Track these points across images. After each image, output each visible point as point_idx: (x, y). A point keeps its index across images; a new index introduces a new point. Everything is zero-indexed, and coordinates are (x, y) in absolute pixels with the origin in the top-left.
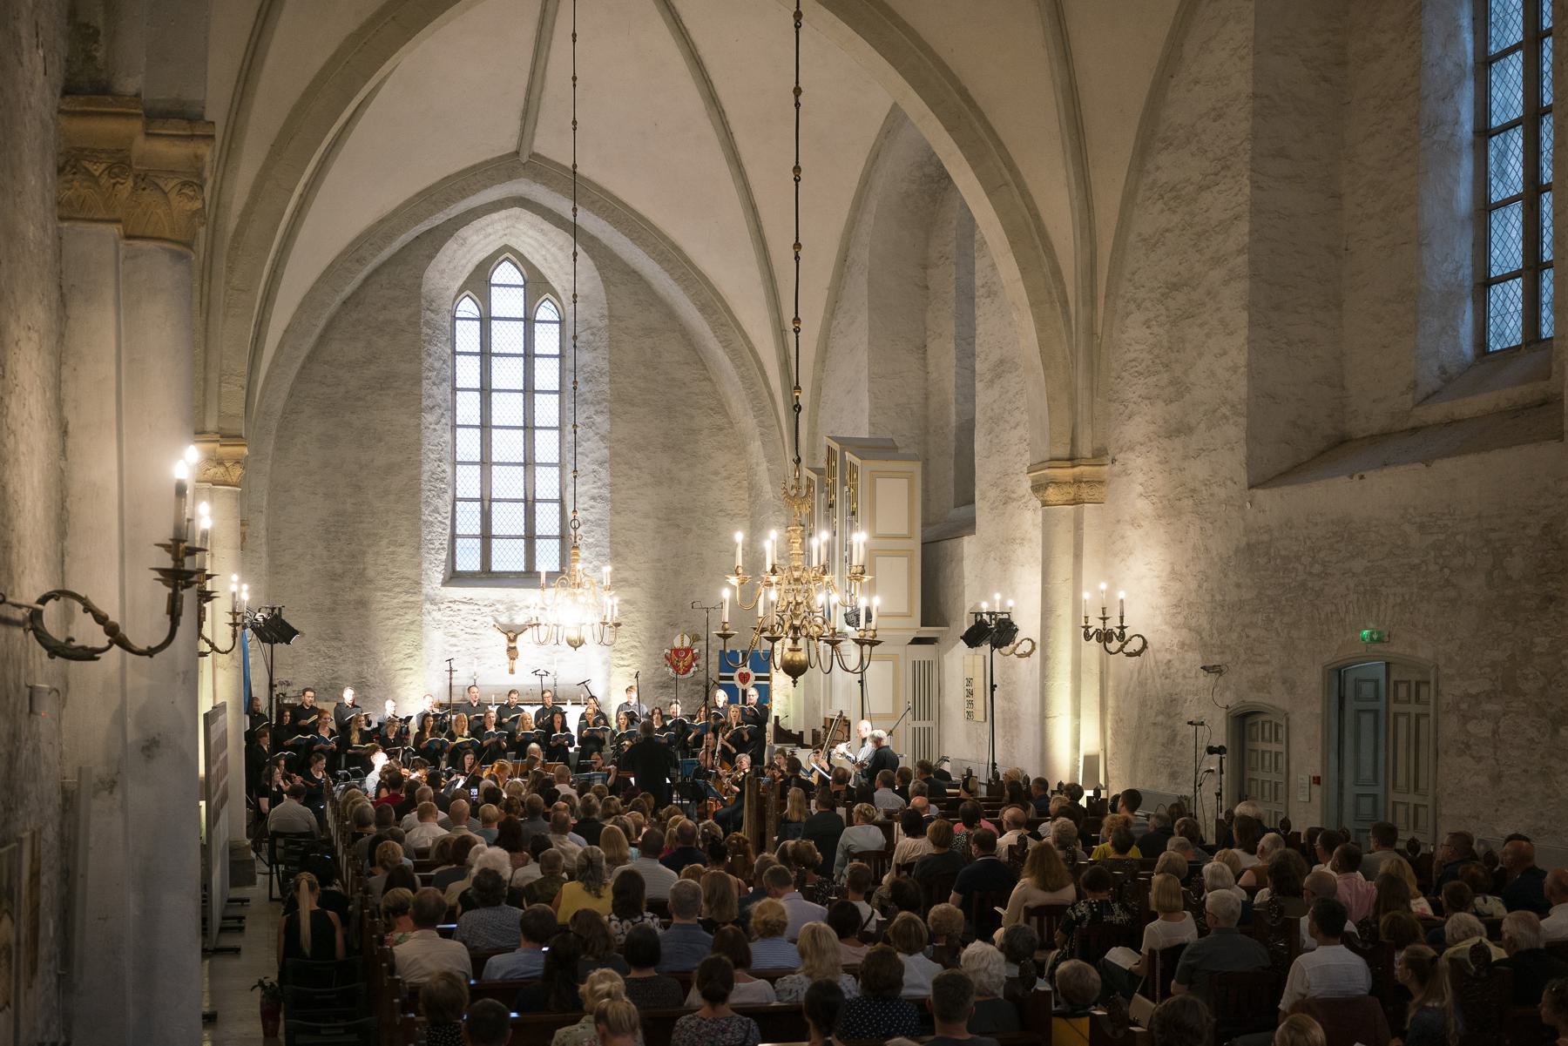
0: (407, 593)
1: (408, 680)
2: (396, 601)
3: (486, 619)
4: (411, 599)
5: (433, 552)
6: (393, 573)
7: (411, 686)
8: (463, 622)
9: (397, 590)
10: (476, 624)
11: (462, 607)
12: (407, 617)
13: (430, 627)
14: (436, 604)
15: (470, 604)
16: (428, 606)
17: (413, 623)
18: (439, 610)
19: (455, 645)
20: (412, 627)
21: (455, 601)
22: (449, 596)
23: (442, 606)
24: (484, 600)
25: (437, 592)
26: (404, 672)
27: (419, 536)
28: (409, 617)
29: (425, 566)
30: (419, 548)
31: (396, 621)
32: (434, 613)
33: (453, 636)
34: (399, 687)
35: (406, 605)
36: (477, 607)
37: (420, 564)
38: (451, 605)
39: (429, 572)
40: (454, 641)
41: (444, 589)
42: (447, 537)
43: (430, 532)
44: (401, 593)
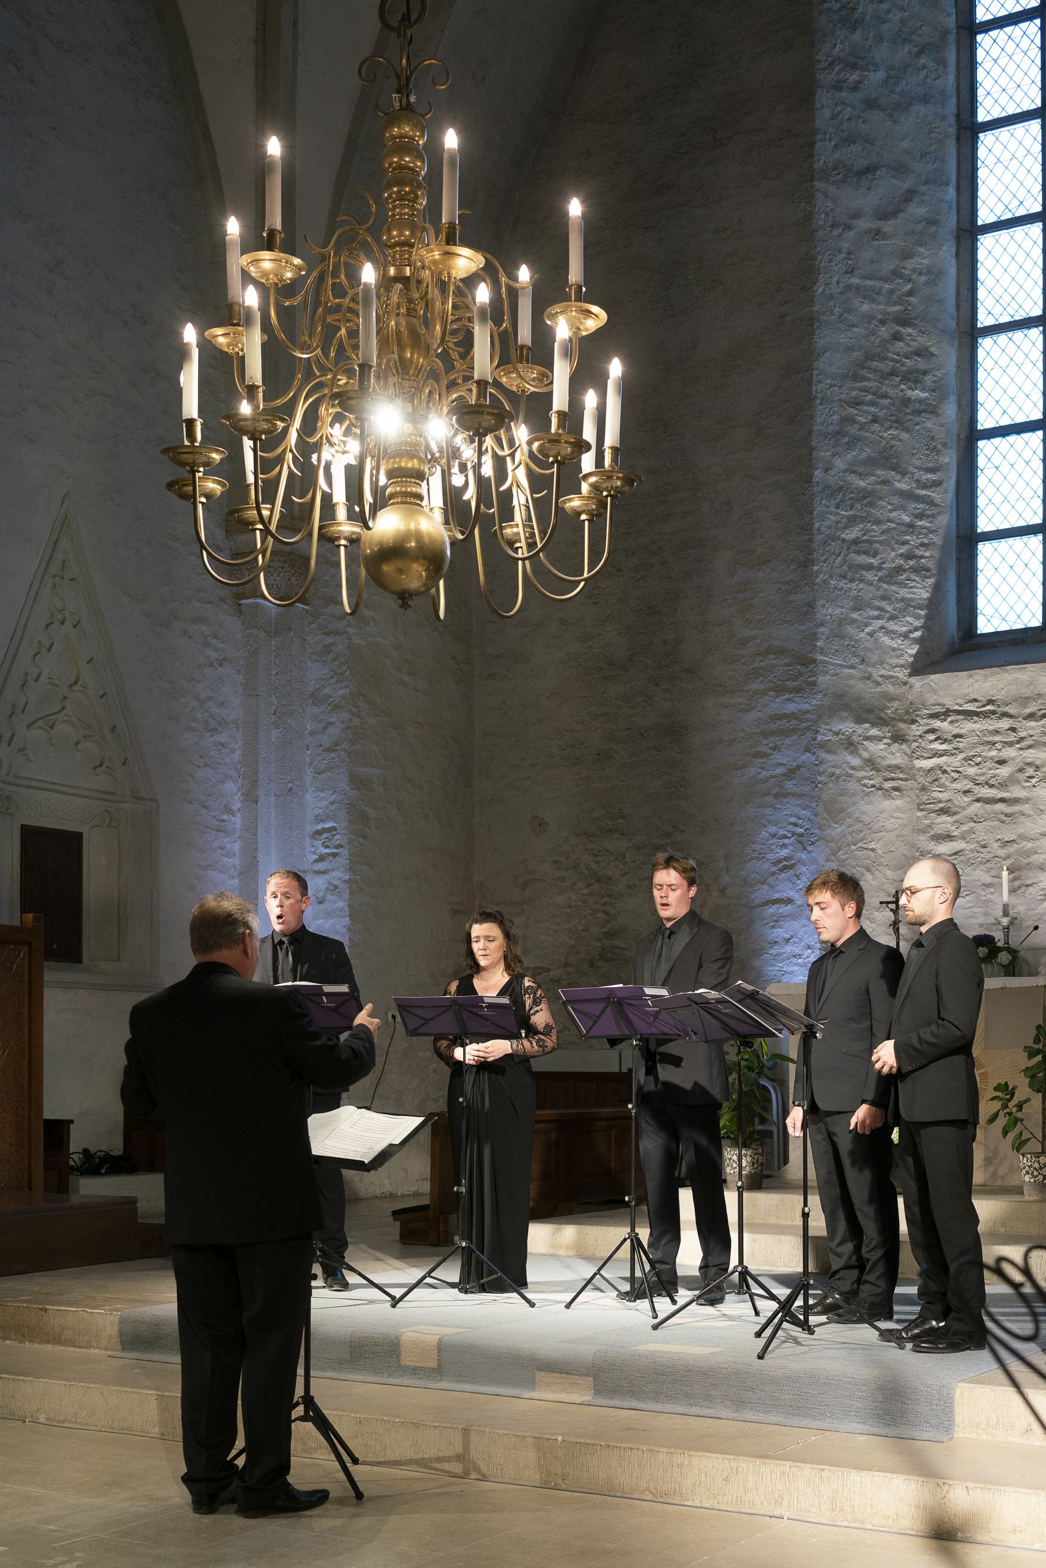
0: (779, 690)
1: (780, 933)
2: (754, 715)
3: (1031, 755)
4: (791, 708)
5: (869, 576)
6: (743, 643)
7: (788, 949)
8: (972, 771)
9: (756, 685)
10: (1004, 771)
11: (968, 726)
12: (778, 757)
13: (852, 785)
14: (881, 722)
15: (986, 715)
16: (848, 727)
17: (792, 772)
18: (898, 738)
19: (948, 837)
20: (790, 785)
21: (947, 713)
22: (932, 699)
23: (916, 730)
24: (1025, 701)
25: (891, 689)
26: (772, 909)
27: (807, 529)
28: (785, 757)
29: (830, 611)
30: (806, 563)
31: (752, 771)
32: (877, 749)
33: (943, 811)
34: (758, 952)
35: (773, 726)
36: (1005, 724)
37: (811, 606)
38: (937, 724)
39: (851, 630)
40: (944, 823)
41: (917, 682)
42: (937, 539)
43: (852, 521)
44: (764, 693)
